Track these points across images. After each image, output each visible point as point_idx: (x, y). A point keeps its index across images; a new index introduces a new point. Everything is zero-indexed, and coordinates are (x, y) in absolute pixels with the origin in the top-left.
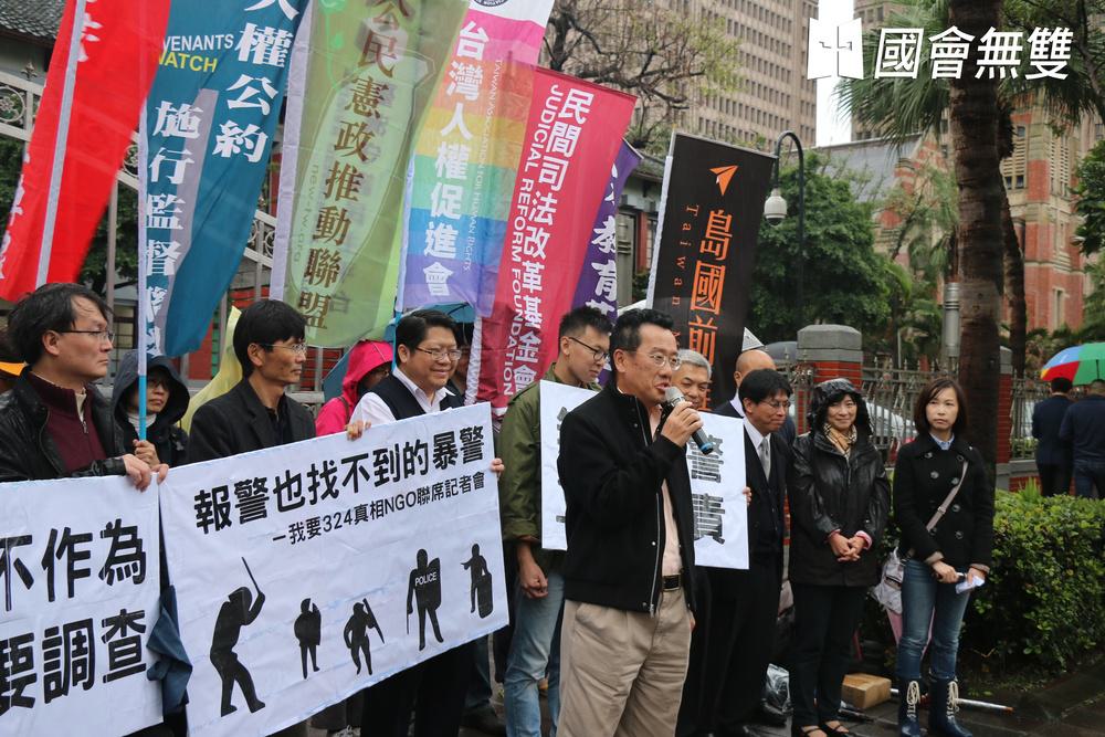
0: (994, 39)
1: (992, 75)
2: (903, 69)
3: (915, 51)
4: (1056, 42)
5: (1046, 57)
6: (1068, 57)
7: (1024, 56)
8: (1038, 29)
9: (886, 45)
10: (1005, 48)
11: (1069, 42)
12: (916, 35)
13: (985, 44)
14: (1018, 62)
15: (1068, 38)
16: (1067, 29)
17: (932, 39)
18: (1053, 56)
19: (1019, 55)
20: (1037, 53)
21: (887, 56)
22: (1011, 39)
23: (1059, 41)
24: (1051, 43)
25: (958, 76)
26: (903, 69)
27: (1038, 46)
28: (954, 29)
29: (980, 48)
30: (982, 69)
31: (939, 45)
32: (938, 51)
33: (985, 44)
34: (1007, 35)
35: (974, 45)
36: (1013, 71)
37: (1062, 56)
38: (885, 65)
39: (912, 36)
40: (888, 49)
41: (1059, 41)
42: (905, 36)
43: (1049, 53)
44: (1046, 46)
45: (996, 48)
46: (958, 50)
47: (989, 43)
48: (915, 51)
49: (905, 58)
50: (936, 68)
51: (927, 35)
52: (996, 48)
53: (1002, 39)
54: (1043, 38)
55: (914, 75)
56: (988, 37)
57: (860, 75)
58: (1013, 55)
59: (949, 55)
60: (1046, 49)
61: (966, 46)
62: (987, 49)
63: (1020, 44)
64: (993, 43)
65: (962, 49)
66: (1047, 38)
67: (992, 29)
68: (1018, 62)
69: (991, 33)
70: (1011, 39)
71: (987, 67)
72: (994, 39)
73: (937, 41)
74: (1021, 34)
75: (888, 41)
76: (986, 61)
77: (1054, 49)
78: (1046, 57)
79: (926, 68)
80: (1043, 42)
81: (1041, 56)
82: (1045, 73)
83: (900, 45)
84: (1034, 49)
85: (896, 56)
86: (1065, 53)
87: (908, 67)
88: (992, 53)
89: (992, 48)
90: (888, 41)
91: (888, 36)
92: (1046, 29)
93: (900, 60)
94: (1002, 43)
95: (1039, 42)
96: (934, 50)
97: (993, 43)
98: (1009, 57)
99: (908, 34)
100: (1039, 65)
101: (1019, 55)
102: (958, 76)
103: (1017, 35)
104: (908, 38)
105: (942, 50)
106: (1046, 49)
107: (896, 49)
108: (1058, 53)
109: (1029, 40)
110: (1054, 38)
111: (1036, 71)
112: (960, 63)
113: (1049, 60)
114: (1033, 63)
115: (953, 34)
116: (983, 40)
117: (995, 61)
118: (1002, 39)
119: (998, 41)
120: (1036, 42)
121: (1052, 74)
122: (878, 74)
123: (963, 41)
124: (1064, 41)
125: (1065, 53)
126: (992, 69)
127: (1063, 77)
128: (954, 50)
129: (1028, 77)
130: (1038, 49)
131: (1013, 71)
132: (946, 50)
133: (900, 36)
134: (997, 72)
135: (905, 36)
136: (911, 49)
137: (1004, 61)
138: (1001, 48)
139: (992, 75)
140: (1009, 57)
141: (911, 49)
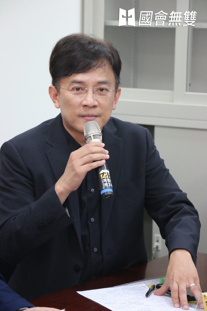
4: (192, 15)
5: (189, 19)
6: (195, 19)
11: (196, 15)
15: (195, 14)
16: (195, 12)
17: (155, 14)
18: (191, 19)
21: (142, 19)
23: (193, 15)
24: (190, 15)
28: (162, 11)
29: (170, 17)
34: (177, 13)
35: (168, 16)
37: (193, 19)
39: (149, 13)
40: (143, 17)
41: (193, 15)
42: (147, 14)
43: (190, 18)
44: (189, 16)
45: (174, 17)
46: (163, 18)
47: (172, 15)
49: (147, 20)
52: (174, 17)
56: (172, 14)
59: (160, 19)
60: (189, 17)
61: (165, 16)
62: (172, 17)
66: (189, 14)
67: (173, 11)
69: (173, 12)
73: (158, 15)
74: (181, 13)
75: (142, 15)
76: (171, 21)
77: (191, 17)
78: (189, 19)
80: (188, 15)
81: (187, 19)
82: (189, 24)
84: (185, 17)
85: (145, 19)
86: (195, 18)
87: (148, 22)
89: (173, 17)
91: (142, 13)
94: (176, 16)
95: (187, 15)
96: (156, 18)
100: (187, 22)
105: (158, 18)
106: (189, 17)
107: (145, 17)
108: (192, 18)
109: (184, 15)
110: (191, 14)
112: (164, 21)
113: (190, 20)
114: (185, 21)
116: (170, 15)
117: (174, 21)
119: (175, 15)
120: (186, 15)
121: (191, 24)
124: (194, 15)
125: (195, 18)
126: (173, 23)
128: (162, 17)
130: (186, 17)
131: (179, 23)
133: (146, 13)
135: (147, 14)
136: (149, 17)
141: (149, 17)
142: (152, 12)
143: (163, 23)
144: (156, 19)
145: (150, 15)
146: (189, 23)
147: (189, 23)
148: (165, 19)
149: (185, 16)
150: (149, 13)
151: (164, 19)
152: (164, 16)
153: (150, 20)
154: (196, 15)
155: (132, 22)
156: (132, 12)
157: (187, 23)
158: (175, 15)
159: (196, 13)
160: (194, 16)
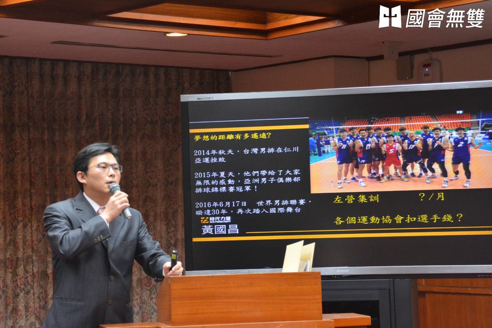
0: (453, 13)
1: (452, 26)
2: (417, 24)
5: (474, 19)
6: (483, 20)
7: (465, 19)
8: (471, 9)
9: (410, 15)
10: (458, 17)
11: (483, 14)
12: (423, 12)
13: (450, 15)
14: (463, 22)
15: (482, 13)
16: (482, 10)
17: (429, 13)
20: (470, 18)
21: (411, 19)
22: (460, 13)
23: (479, 14)
25: (439, 26)
26: (417, 24)
27: (471, 16)
28: (437, 9)
29: (448, 17)
30: (448, 24)
31: (431, 15)
32: (431, 17)
33: (450, 15)
34: (458, 12)
35: (445, 16)
37: (480, 19)
38: (410, 23)
39: (421, 12)
40: (411, 17)
41: (479, 14)
42: (418, 12)
43: (475, 18)
44: (474, 16)
45: (454, 16)
49: (418, 20)
50: (430, 24)
52: (454, 16)
53: (457, 13)
54: (473, 13)
55: (422, 26)
57: (400, 26)
58: (461, 19)
59: (436, 19)
61: (442, 16)
62: (451, 17)
63: (464, 14)
64: (453, 15)
65: (441, 17)
66: (474, 13)
67: (453, 9)
68: (463, 22)
69: (452, 11)
70: (460, 13)
71: (451, 23)
72: (453, 13)
73: (432, 14)
74: (464, 11)
76: (450, 21)
77: (477, 17)
78: (474, 19)
79: (426, 22)
80: (473, 14)
82: (473, 26)
83: (416, 15)
84: (469, 17)
87: (419, 23)
88: (452, 18)
89: (453, 17)
90: (411, 14)
91: (411, 12)
92: (474, 10)
93: (416, 21)
94: (456, 15)
97: (453, 15)
98: (459, 18)
99: (419, 11)
100: (471, 22)
102: (439, 26)
103: (462, 12)
104: (419, 13)
105: (432, 17)
107: (414, 17)
108: (479, 18)
110: (477, 13)
111: (470, 24)
112: (440, 22)
113: (475, 20)
114: (469, 22)
115: (437, 11)
116: (449, 13)
117: (454, 21)
118: (457, 13)
119: (455, 14)
121: (476, 26)
122: (407, 26)
123: (441, 14)
124: (481, 14)
126: (452, 24)
127: (481, 27)
128: (437, 17)
129: (467, 27)
132: (434, 17)
133: (416, 12)
134: (455, 25)
135: (418, 12)
136: (420, 17)
137: (457, 21)
138: (456, 17)
139: (452, 26)
141: (420, 17)
142: (424, 10)
143: (439, 24)
144: (429, 19)
148: (442, 19)
149: (469, 15)
150: (421, 12)
151: (440, 19)
152: (440, 15)
153: (421, 20)
154: (483, 14)
156: (397, 10)
157: (472, 24)
158: (455, 14)
159: (484, 11)
160: (480, 16)
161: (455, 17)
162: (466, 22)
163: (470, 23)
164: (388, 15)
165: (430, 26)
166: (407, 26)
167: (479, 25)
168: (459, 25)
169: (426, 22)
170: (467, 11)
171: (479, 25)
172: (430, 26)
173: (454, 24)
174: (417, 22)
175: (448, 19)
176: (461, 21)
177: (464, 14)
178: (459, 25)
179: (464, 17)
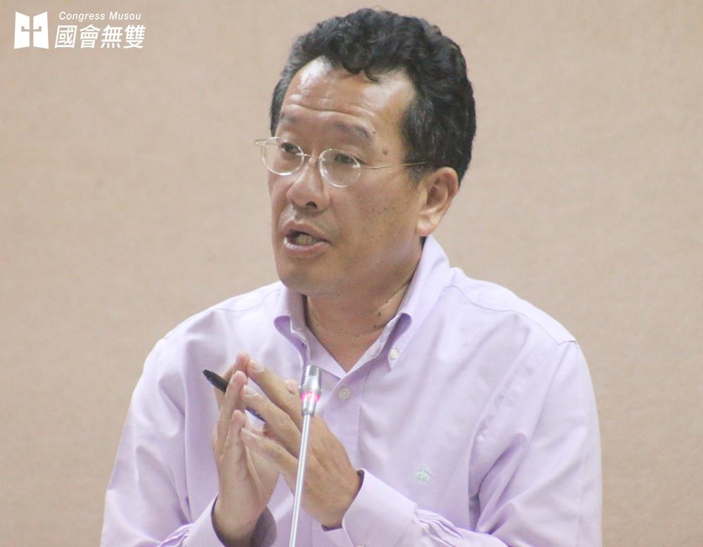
0: (109, 30)
1: (108, 47)
2: (68, 44)
3: (73, 36)
4: (137, 31)
6: (143, 38)
9: (60, 33)
10: (115, 34)
14: (120, 41)
17: (81, 30)
18: (137, 38)
19: (121, 37)
21: (61, 38)
25: (93, 47)
28: (91, 26)
29: (103, 34)
30: (104, 44)
34: (115, 29)
35: (100, 33)
36: (118, 44)
37: (140, 38)
38: (60, 42)
43: (135, 36)
45: (111, 34)
48: (73, 36)
49: (69, 39)
50: (83, 43)
51: (78, 29)
52: (111, 34)
53: (113, 31)
55: (73, 46)
57: (47, 47)
58: (118, 38)
59: (89, 37)
61: (97, 34)
62: (106, 35)
63: (122, 31)
65: (95, 35)
67: (109, 26)
68: (120, 41)
69: (108, 27)
71: (106, 43)
72: (109, 30)
73: (84, 31)
74: (121, 28)
76: (106, 40)
77: (137, 35)
79: (78, 42)
80: (132, 32)
81: (131, 38)
82: (133, 46)
84: (128, 35)
85: (64, 38)
87: (70, 43)
88: (108, 36)
91: (61, 29)
93: (66, 40)
94: (113, 32)
98: (116, 38)
100: (130, 42)
101: (121, 37)
102: (93, 47)
103: (120, 29)
109: (126, 31)
110: (137, 30)
111: (128, 44)
112: (94, 41)
114: (127, 41)
115: (90, 28)
117: (110, 40)
118: (113, 31)
119: (111, 31)
121: (136, 46)
122: (56, 46)
123: (95, 31)
124: (141, 31)
126: (108, 44)
127: (141, 47)
128: (91, 35)
129: (125, 47)
131: (118, 44)
132: (87, 35)
133: (66, 29)
134: (111, 45)
136: (72, 35)
137: (114, 40)
139: (108, 47)
140: (116, 38)
142: (76, 27)
143: (93, 44)
144: (82, 37)
145: (72, 31)
146: (133, 43)
147: (133, 43)
148: (96, 38)
153: (72, 38)
155: (42, 41)
158: (111, 31)
161: (112, 35)
162: (124, 42)
163: (128, 43)
164: (35, 33)
165: (82, 47)
166: (56, 46)
167: (140, 45)
168: (116, 46)
169: (78, 42)
170: (125, 27)
171: (140, 45)
172: (82, 47)
173: (111, 43)
174: (68, 41)
175: (104, 37)
176: (118, 40)
177: (122, 31)
178: (116, 46)
179: (121, 34)
